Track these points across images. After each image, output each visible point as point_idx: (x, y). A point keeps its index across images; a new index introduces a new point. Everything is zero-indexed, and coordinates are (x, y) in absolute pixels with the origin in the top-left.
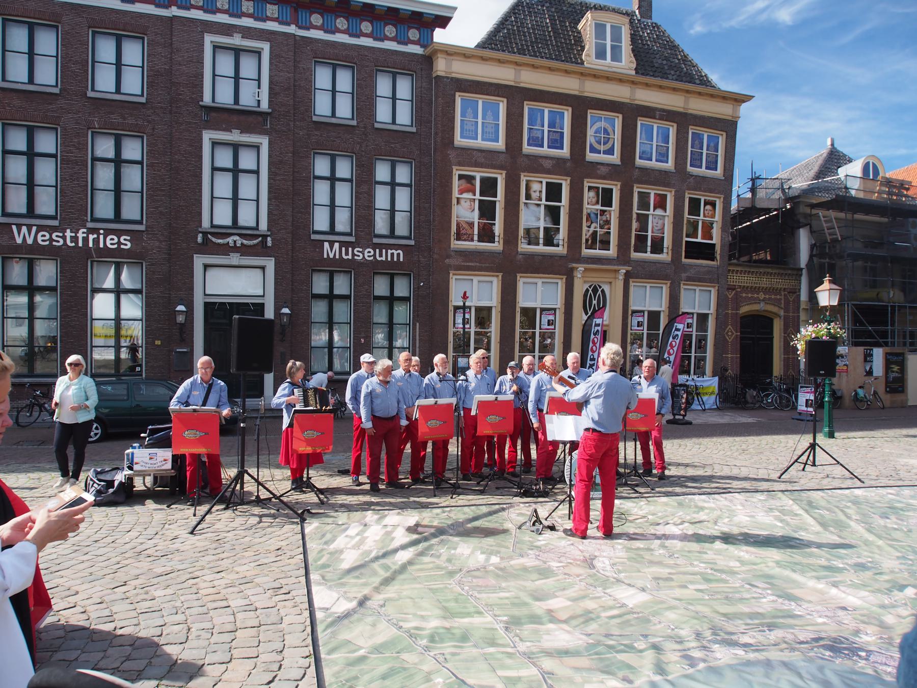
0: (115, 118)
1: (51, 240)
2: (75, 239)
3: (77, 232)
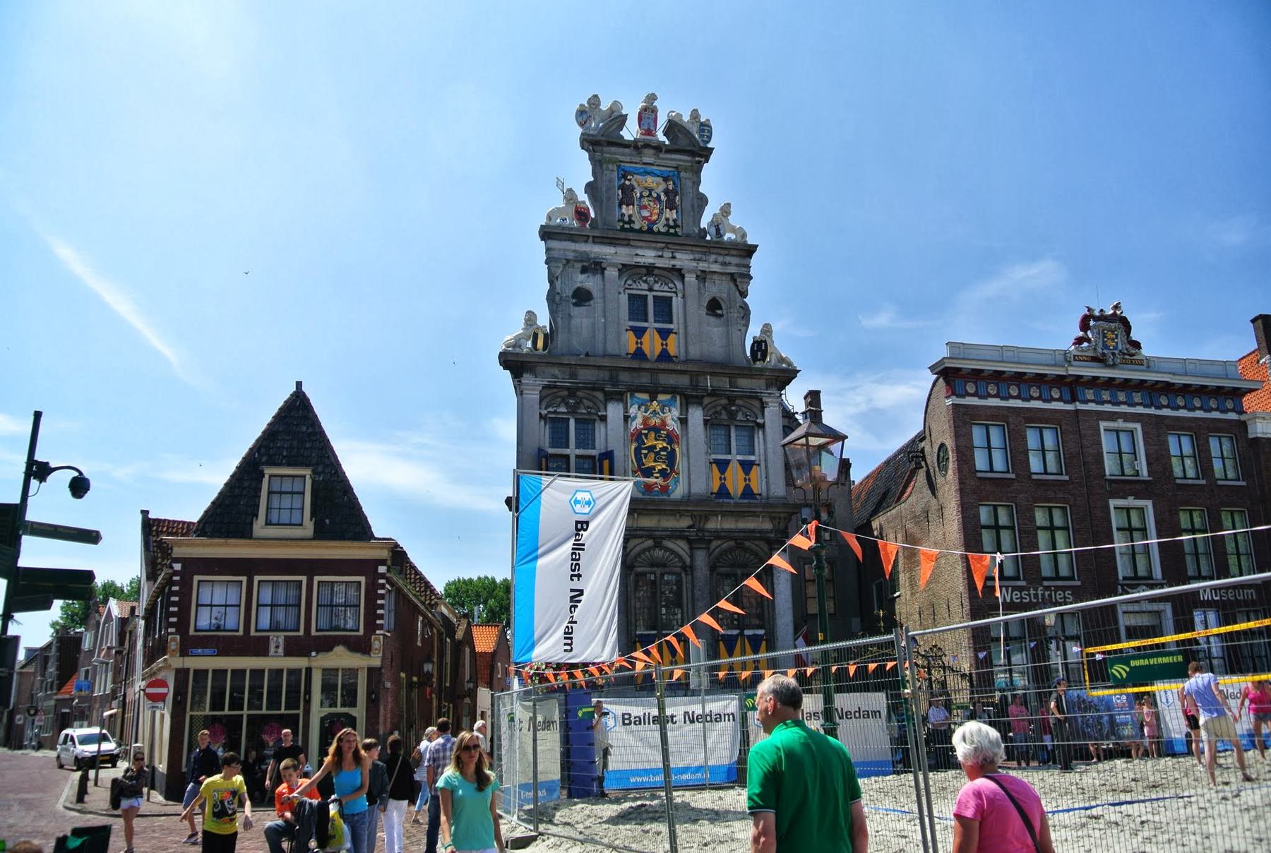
0: (1050, 494)
1: (1021, 598)
2: (1036, 596)
3: (1036, 589)
